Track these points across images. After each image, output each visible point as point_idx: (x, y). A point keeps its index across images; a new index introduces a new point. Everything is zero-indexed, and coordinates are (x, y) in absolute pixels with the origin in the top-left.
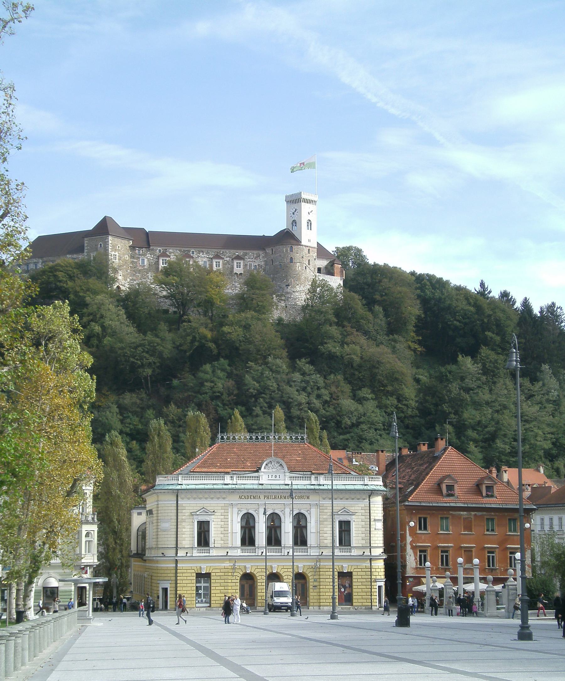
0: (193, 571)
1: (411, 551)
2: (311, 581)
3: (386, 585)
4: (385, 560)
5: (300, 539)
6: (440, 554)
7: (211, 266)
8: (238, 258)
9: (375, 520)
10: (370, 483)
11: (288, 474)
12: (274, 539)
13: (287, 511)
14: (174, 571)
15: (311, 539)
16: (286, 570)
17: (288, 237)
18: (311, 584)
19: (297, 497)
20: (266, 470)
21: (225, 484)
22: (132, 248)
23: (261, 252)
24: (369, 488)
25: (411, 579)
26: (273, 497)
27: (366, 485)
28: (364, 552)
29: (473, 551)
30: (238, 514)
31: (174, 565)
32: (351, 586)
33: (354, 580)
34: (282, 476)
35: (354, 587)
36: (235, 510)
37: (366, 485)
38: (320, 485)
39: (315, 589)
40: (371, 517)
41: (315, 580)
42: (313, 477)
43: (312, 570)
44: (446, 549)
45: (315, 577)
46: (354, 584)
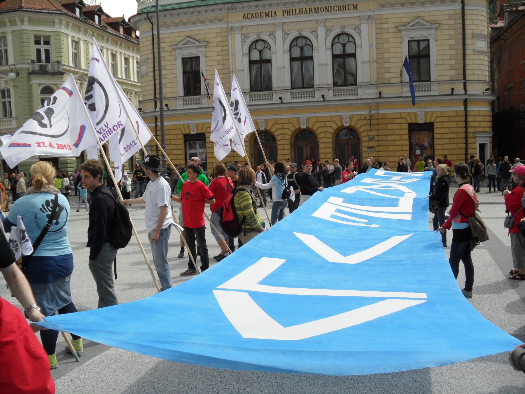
0: (179, 132)
2: (364, 139)
3: (494, 143)
4: (492, 104)
5: (344, 73)
9: (473, 36)
13: (321, 31)
15: (364, 72)
16: (322, 124)
18: (364, 144)
19: (336, 8)
26: (298, 11)
28: (453, 90)
30: (243, 42)
32: (432, 145)
33: (436, 136)
35: (436, 147)
36: (238, 37)
40: (467, 32)
41: (371, 139)
43: (365, 122)
46: (436, 142)
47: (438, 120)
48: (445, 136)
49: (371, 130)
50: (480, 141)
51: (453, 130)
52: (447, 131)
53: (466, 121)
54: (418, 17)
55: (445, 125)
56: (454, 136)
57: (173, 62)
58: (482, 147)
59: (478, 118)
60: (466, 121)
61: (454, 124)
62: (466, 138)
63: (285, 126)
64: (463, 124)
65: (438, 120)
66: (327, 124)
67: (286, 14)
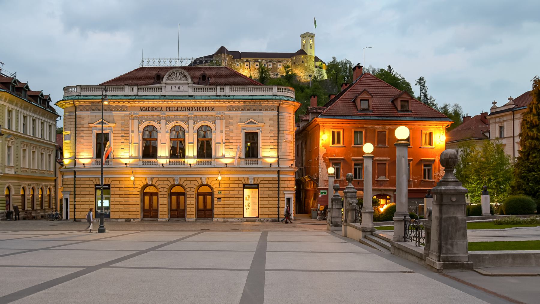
1: (324, 164)
6: (353, 167)
7: (268, 66)
8: (280, 62)
10: (279, 94)
11: (191, 85)
12: (177, 152)
14: (73, 183)
16: (189, 182)
17: (302, 52)
19: (201, 109)
20: (167, 82)
21: (125, 96)
22: (234, 58)
23: (290, 59)
24: (277, 98)
25: (323, 192)
26: (176, 109)
27: (274, 96)
29: (387, 164)
31: (73, 177)
34: (186, 87)
37: (274, 96)
38: (226, 96)
39: (220, 201)
42: (218, 87)
44: (360, 162)
45: (220, 189)
47: (262, 182)
48: (265, 192)
49: (220, 187)
50: (287, 196)
51: (270, 189)
52: (267, 189)
53: (279, 184)
54: (251, 118)
55: (266, 186)
56: (271, 192)
57: (90, 135)
58: (289, 200)
59: (286, 182)
60: (279, 184)
61: (271, 185)
62: (279, 194)
63: (165, 182)
64: (277, 185)
65: (262, 182)
66: (192, 182)
67: (168, 110)
